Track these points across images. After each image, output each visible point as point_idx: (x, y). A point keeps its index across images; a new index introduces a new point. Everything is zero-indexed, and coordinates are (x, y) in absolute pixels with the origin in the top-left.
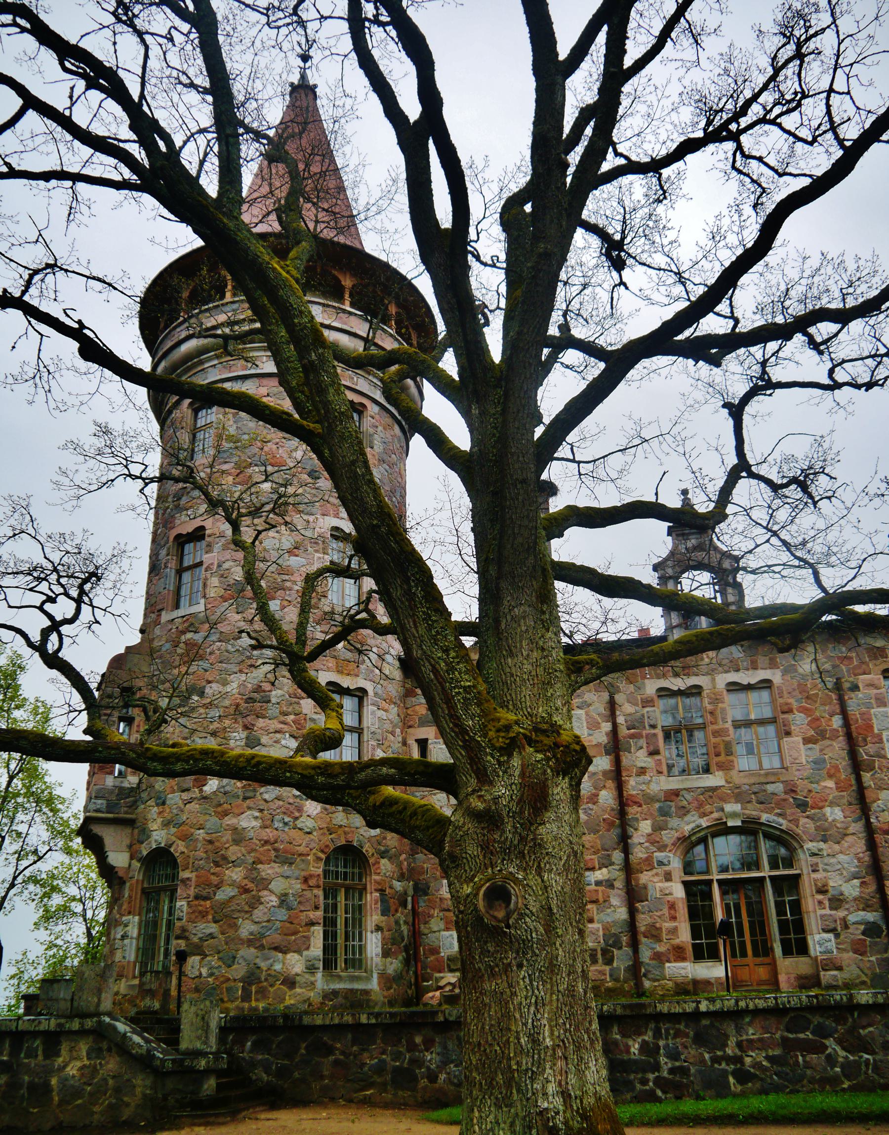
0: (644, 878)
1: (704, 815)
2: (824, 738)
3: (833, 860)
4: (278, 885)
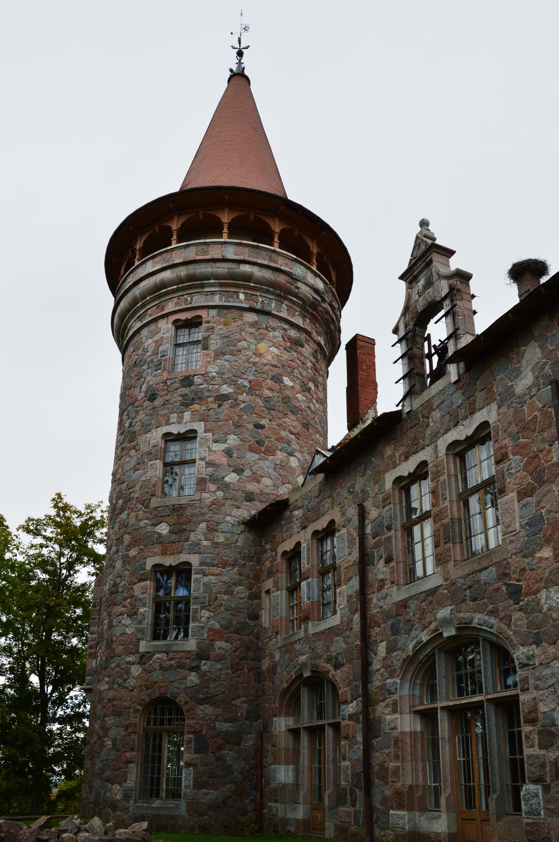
1: (425, 627)
2: (542, 483)
3: (547, 672)
4: (113, 732)
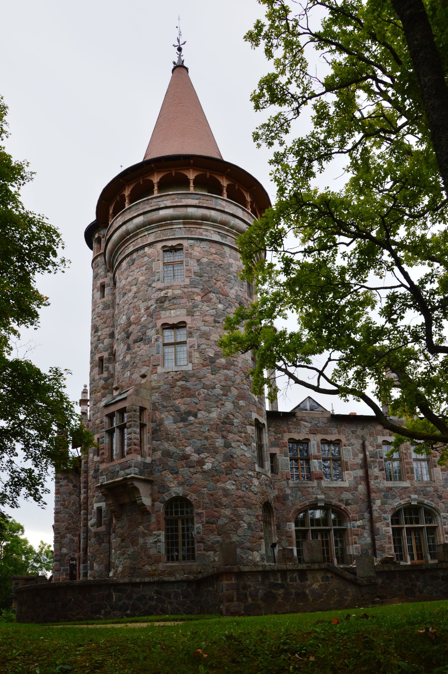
0: (378, 525)
1: (402, 499)
